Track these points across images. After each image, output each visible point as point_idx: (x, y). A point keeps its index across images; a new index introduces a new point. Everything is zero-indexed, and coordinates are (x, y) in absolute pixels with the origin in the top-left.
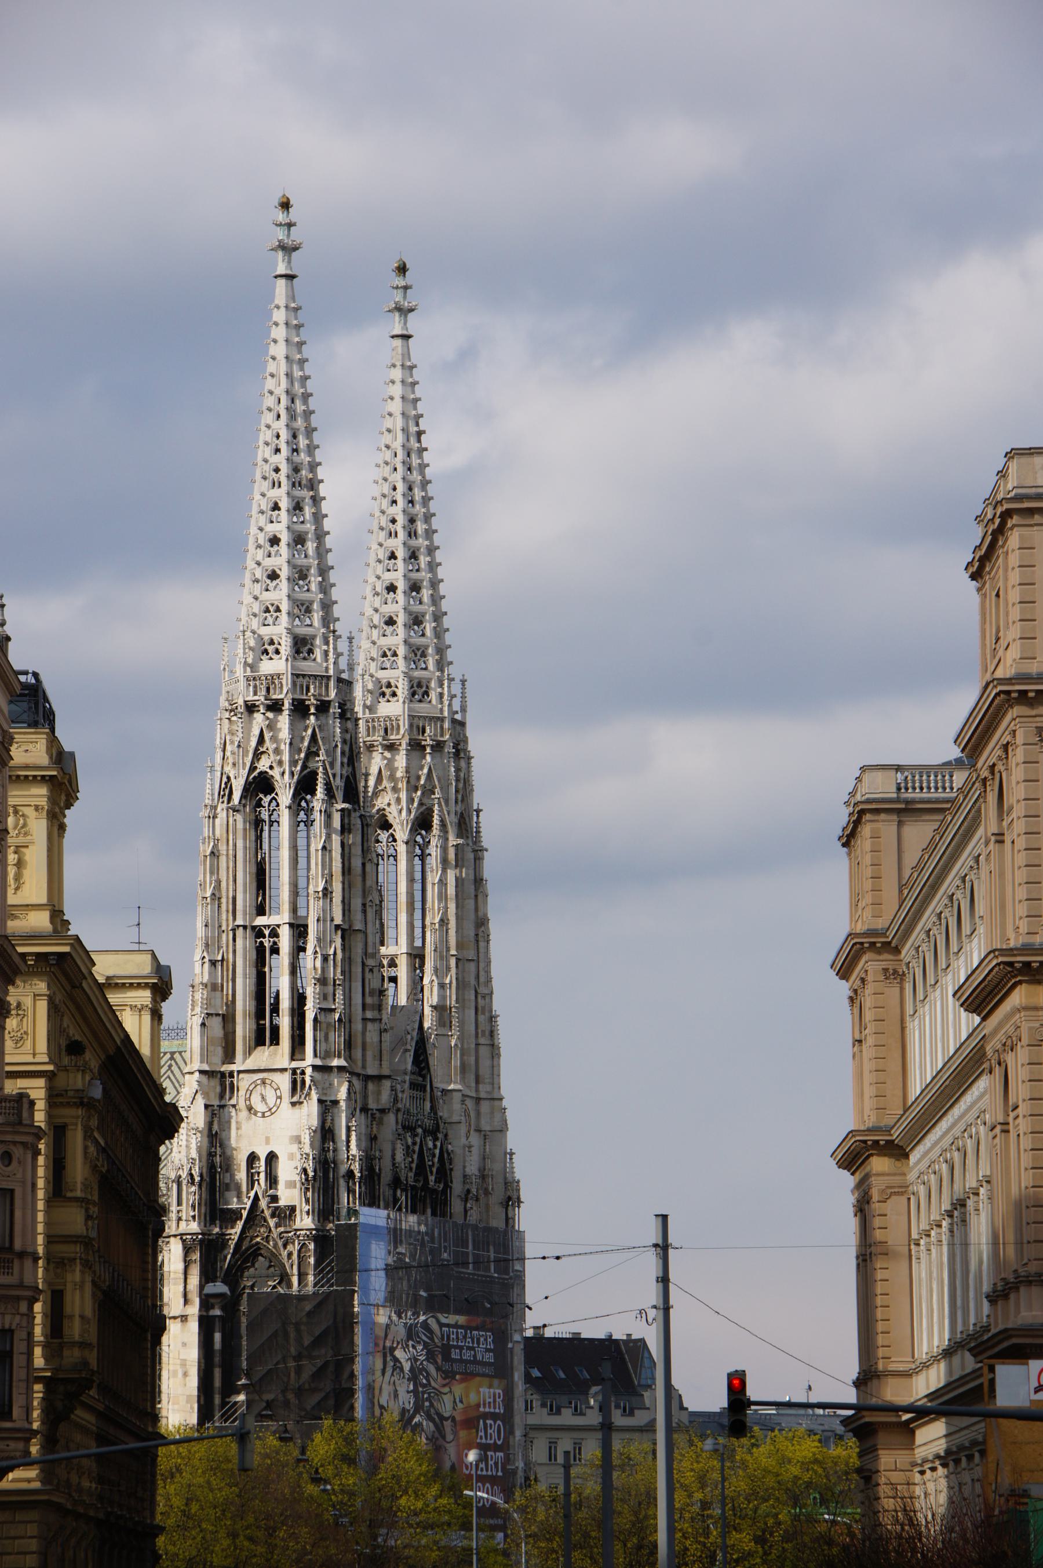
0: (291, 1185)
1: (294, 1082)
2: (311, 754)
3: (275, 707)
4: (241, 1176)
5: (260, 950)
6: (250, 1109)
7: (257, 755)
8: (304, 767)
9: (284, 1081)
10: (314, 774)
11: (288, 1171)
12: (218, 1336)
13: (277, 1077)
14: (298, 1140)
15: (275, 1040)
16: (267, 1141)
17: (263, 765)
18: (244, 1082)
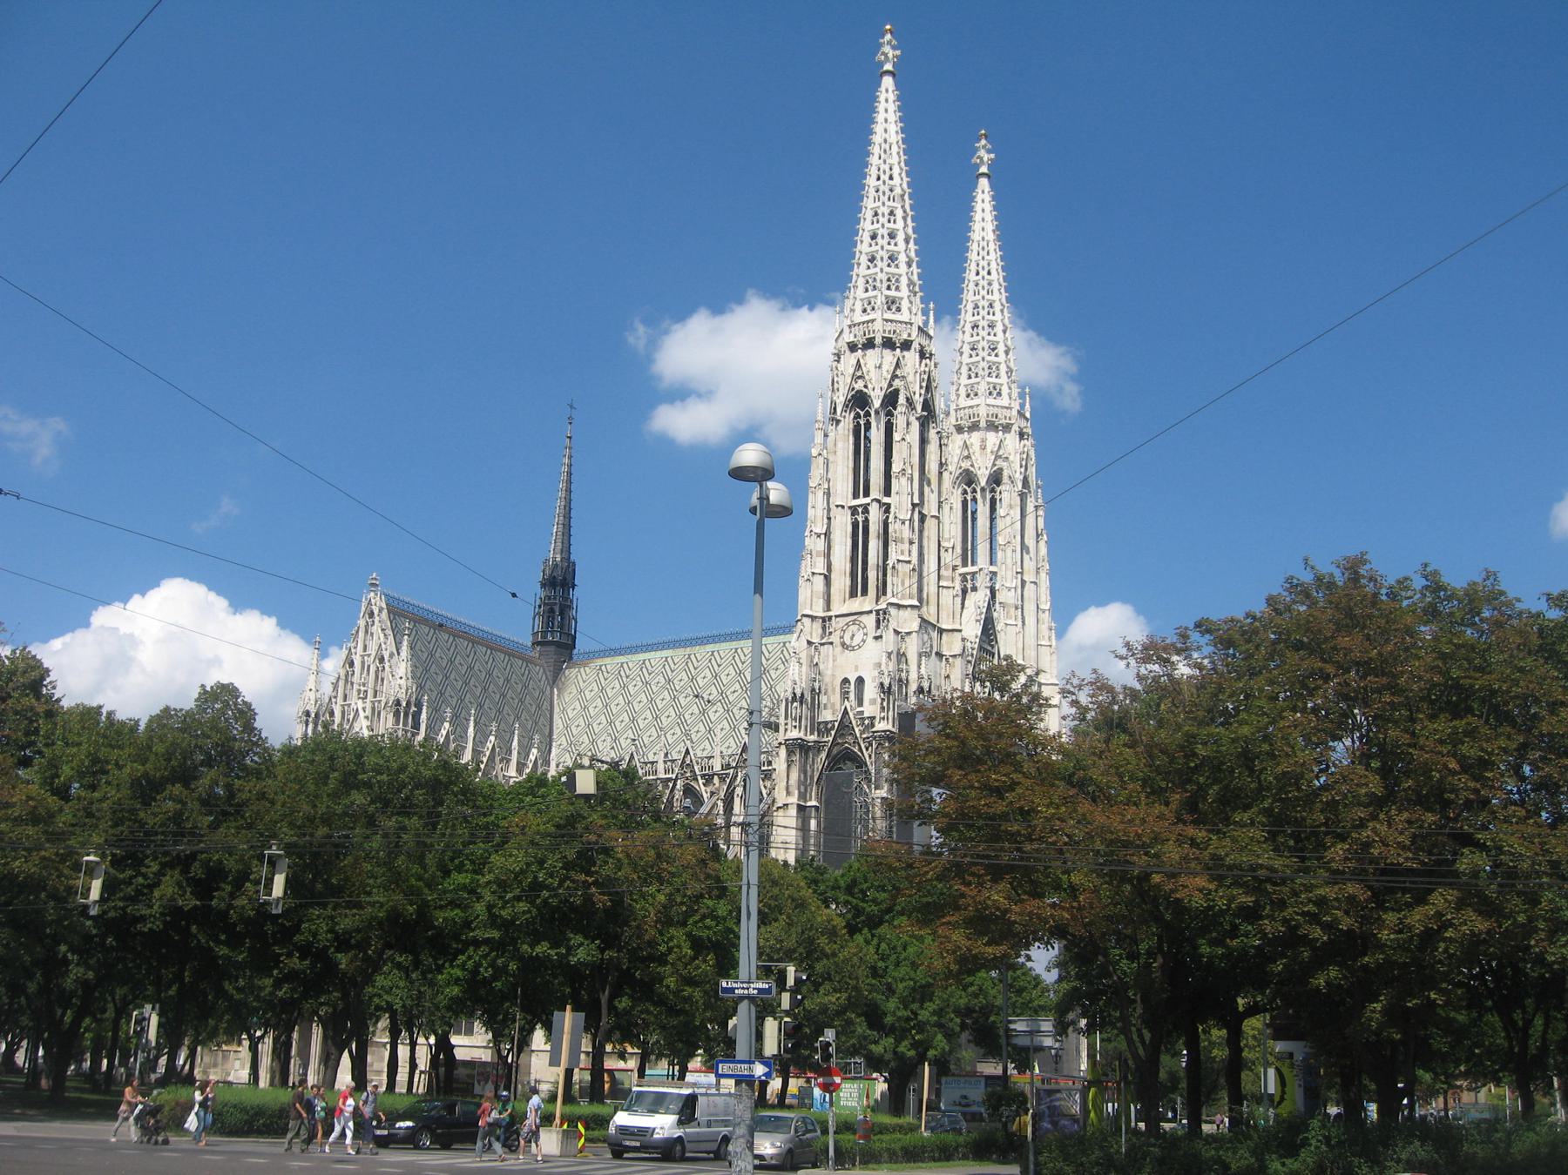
0: (873, 702)
1: (878, 621)
2: (894, 377)
3: (870, 344)
4: (836, 698)
5: (855, 525)
6: (843, 644)
7: (855, 378)
8: (890, 385)
9: (870, 621)
10: (897, 392)
11: (871, 691)
12: (813, 824)
13: (864, 618)
14: (879, 665)
15: (865, 592)
16: (856, 668)
17: (859, 385)
18: (837, 624)
